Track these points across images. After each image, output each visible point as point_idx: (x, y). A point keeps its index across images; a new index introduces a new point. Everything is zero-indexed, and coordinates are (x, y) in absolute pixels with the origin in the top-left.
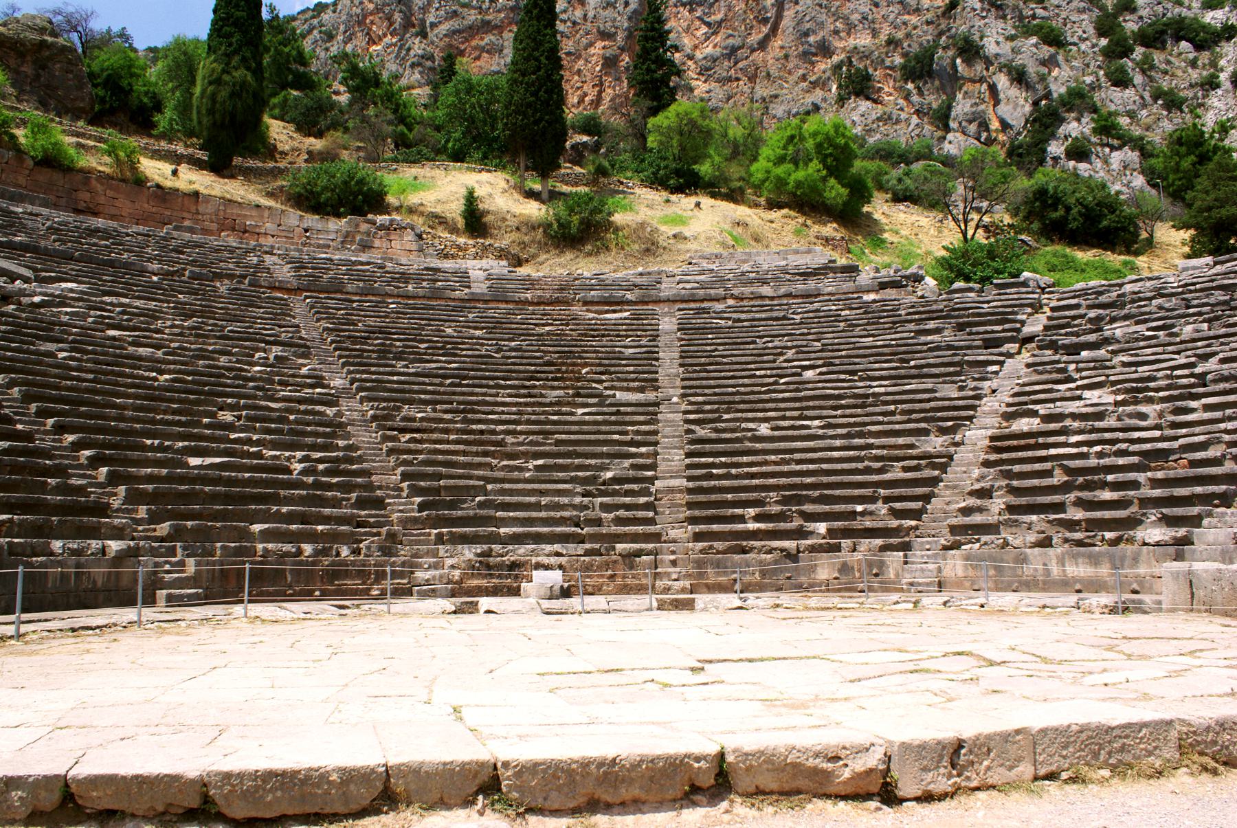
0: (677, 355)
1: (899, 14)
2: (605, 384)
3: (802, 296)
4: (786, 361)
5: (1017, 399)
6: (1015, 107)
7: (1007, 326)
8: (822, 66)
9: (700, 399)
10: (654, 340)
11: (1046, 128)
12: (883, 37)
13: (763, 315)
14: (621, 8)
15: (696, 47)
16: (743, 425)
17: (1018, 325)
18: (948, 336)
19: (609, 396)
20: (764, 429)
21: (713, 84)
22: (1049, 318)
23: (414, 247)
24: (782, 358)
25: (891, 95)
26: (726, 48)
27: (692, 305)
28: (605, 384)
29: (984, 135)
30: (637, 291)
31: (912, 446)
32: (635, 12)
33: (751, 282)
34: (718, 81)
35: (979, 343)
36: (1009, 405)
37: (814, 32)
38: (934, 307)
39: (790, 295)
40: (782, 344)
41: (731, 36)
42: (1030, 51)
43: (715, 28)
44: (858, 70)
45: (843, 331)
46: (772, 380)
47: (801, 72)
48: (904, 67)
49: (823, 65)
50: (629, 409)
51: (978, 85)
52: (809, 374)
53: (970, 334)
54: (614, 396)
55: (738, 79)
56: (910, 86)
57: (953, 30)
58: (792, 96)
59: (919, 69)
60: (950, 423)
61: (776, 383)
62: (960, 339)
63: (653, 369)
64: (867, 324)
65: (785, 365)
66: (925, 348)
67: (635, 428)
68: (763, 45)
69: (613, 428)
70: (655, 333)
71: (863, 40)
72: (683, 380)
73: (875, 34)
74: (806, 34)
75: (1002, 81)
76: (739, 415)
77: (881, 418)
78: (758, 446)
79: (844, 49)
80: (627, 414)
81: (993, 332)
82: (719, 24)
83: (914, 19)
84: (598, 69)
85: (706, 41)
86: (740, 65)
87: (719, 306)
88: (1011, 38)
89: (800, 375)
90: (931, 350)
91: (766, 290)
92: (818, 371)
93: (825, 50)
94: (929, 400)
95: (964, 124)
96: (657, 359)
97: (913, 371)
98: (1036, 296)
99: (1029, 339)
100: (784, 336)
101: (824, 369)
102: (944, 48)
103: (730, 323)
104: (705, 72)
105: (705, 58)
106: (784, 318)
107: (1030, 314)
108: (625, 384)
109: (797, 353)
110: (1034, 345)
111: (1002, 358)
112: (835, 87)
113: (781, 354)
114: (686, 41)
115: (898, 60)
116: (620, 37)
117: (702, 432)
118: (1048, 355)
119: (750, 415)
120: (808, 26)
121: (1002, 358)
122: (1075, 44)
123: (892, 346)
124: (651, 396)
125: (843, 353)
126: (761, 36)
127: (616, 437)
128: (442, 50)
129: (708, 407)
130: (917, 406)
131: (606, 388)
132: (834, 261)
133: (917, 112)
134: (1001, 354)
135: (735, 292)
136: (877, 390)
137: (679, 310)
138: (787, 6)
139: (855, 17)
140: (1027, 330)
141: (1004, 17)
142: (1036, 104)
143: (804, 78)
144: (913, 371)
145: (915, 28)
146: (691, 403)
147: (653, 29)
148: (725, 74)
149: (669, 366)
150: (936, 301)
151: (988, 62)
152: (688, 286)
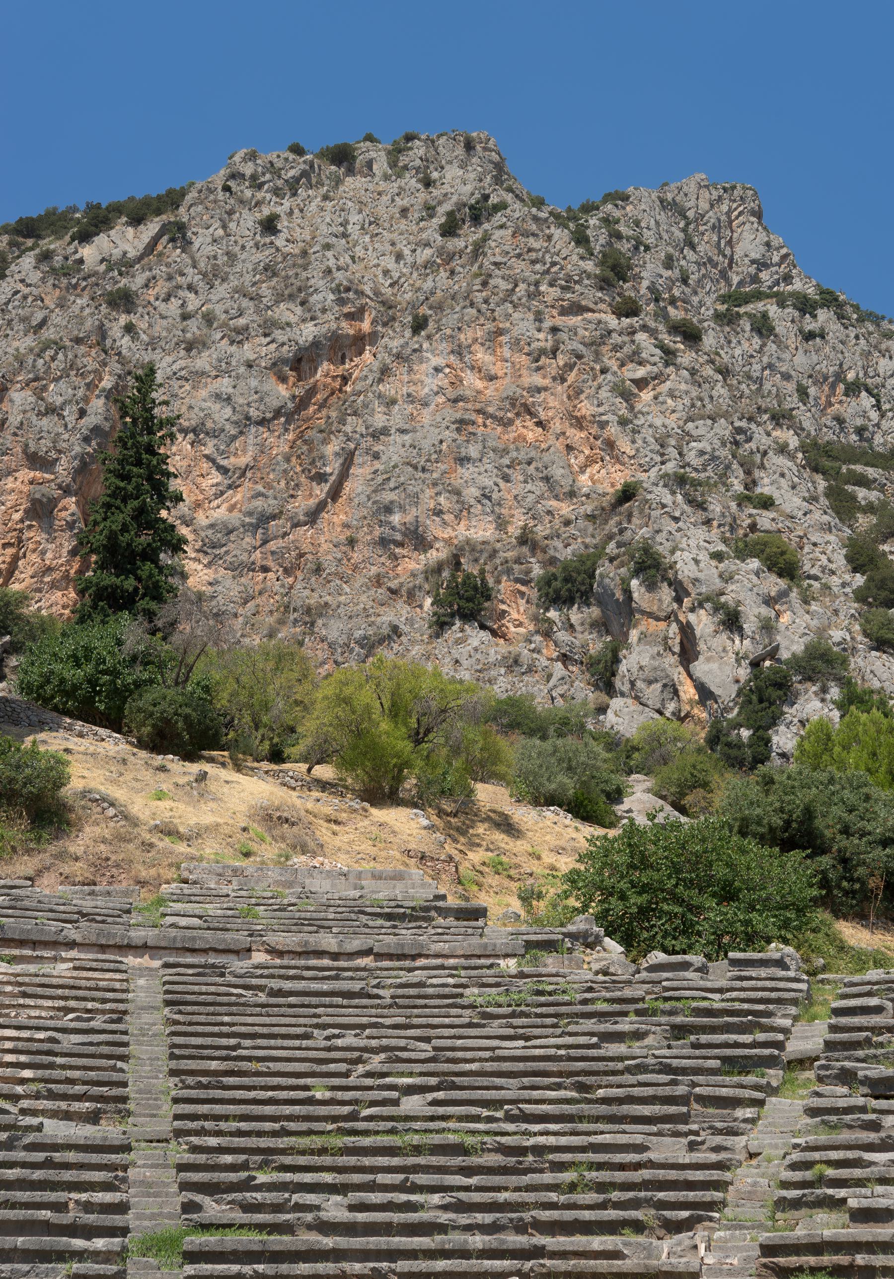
0: (162, 1051)
1: (541, 497)
2: (25, 1104)
3: (390, 956)
4: (369, 1075)
5: (798, 1176)
6: (723, 667)
7: (761, 1037)
8: (412, 565)
9: (213, 1141)
10: (119, 1021)
11: (771, 704)
12: (514, 530)
13: (325, 987)
14: (71, 419)
15: (198, 505)
16: (296, 1198)
17: (780, 1037)
18: (654, 1046)
19: (29, 1129)
20: (335, 1208)
21: (222, 571)
22: (833, 1029)
24: (361, 1069)
25: (520, 625)
26: (250, 514)
27: (190, 959)
28: (25, 1104)
29: (671, 707)
30: (83, 924)
31: (616, 1255)
32: (96, 430)
33: (300, 923)
35: (714, 1064)
36: (785, 1185)
37: (402, 509)
38: (628, 993)
39: (368, 952)
40: (362, 1043)
41: (260, 494)
42: (749, 584)
43: (233, 478)
44: (468, 576)
45: (470, 1025)
46: (346, 1110)
47: (374, 570)
48: (548, 581)
49: (413, 564)
50: (72, 1156)
51: (662, 625)
52: (412, 1104)
53: (696, 1046)
54: (39, 1128)
55: (265, 569)
56: (552, 614)
57: (629, 533)
58: (353, 608)
59: (568, 587)
60: (685, 1214)
61: (353, 1117)
62: (680, 1053)
63: (115, 1076)
64: (513, 1015)
65: (369, 1082)
66: (620, 1066)
67: (84, 1196)
68: (313, 516)
69: (38, 1196)
70: (121, 1007)
71: (481, 530)
72: (176, 1101)
73: (502, 524)
74: (388, 509)
75: (703, 622)
76: (288, 1177)
77: (553, 1196)
78: (329, 1242)
79: (448, 542)
80: (67, 1166)
81: (737, 1045)
83: (565, 509)
84: (17, 516)
85: (217, 496)
86: (272, 545)
87: (238, 965)
88: (718, 556)
89: (396, 1103)
90: (628, 1070)
91: (328, 941)
92: (430, 1097)
93: (419, 540)
94: (637, 1166)
95: (640, 684)
96: (123, 1058)
97: (603, 1109)
98: (803, 986)
99: (803, 1062)
101: (440, 1095)
102: (611, 560)
103: (262, 998)
104: (210, 549)
105: (212, 526)
106: (362, 994)
107: (796, 1018)
108: (63, 1105)
109: (390, 1060)
110: (810, 1074)
111: (759, 1095)
112: (428, 601)
113: (358, 1061)
115: (537, 571)
116: (64, 469)
117: (213, 1208)
118: (839, 1095)
119: (308, 1178)
121: (759, 1095)
122: (816, 578)
123: (559, 1059)
124: (108, 1130)
125: (474, 1067)
126: (312, 502)
127: (45, 1214)
129: (228, 1159)
130: (620, 1176)
131: (23, 1112)
132: (443, 897)
133: (565, 658)
134: (757, 1087)
135: (274, 939)
136: (541, 1140)
137: (166, 965)
138: (358, 459)
139: (471, 493)
140: (795, 1047)
141: (708, 522)
142: (755, 664)
143: (378, 581)
144: (603, 1109)
145: (567, 523)
146: (195, 1149)
147: (139, 463)
148: (244, 557)
149: (148, 1070)
150: (629, 982)
151: (680, 592)
152: (183, 922)
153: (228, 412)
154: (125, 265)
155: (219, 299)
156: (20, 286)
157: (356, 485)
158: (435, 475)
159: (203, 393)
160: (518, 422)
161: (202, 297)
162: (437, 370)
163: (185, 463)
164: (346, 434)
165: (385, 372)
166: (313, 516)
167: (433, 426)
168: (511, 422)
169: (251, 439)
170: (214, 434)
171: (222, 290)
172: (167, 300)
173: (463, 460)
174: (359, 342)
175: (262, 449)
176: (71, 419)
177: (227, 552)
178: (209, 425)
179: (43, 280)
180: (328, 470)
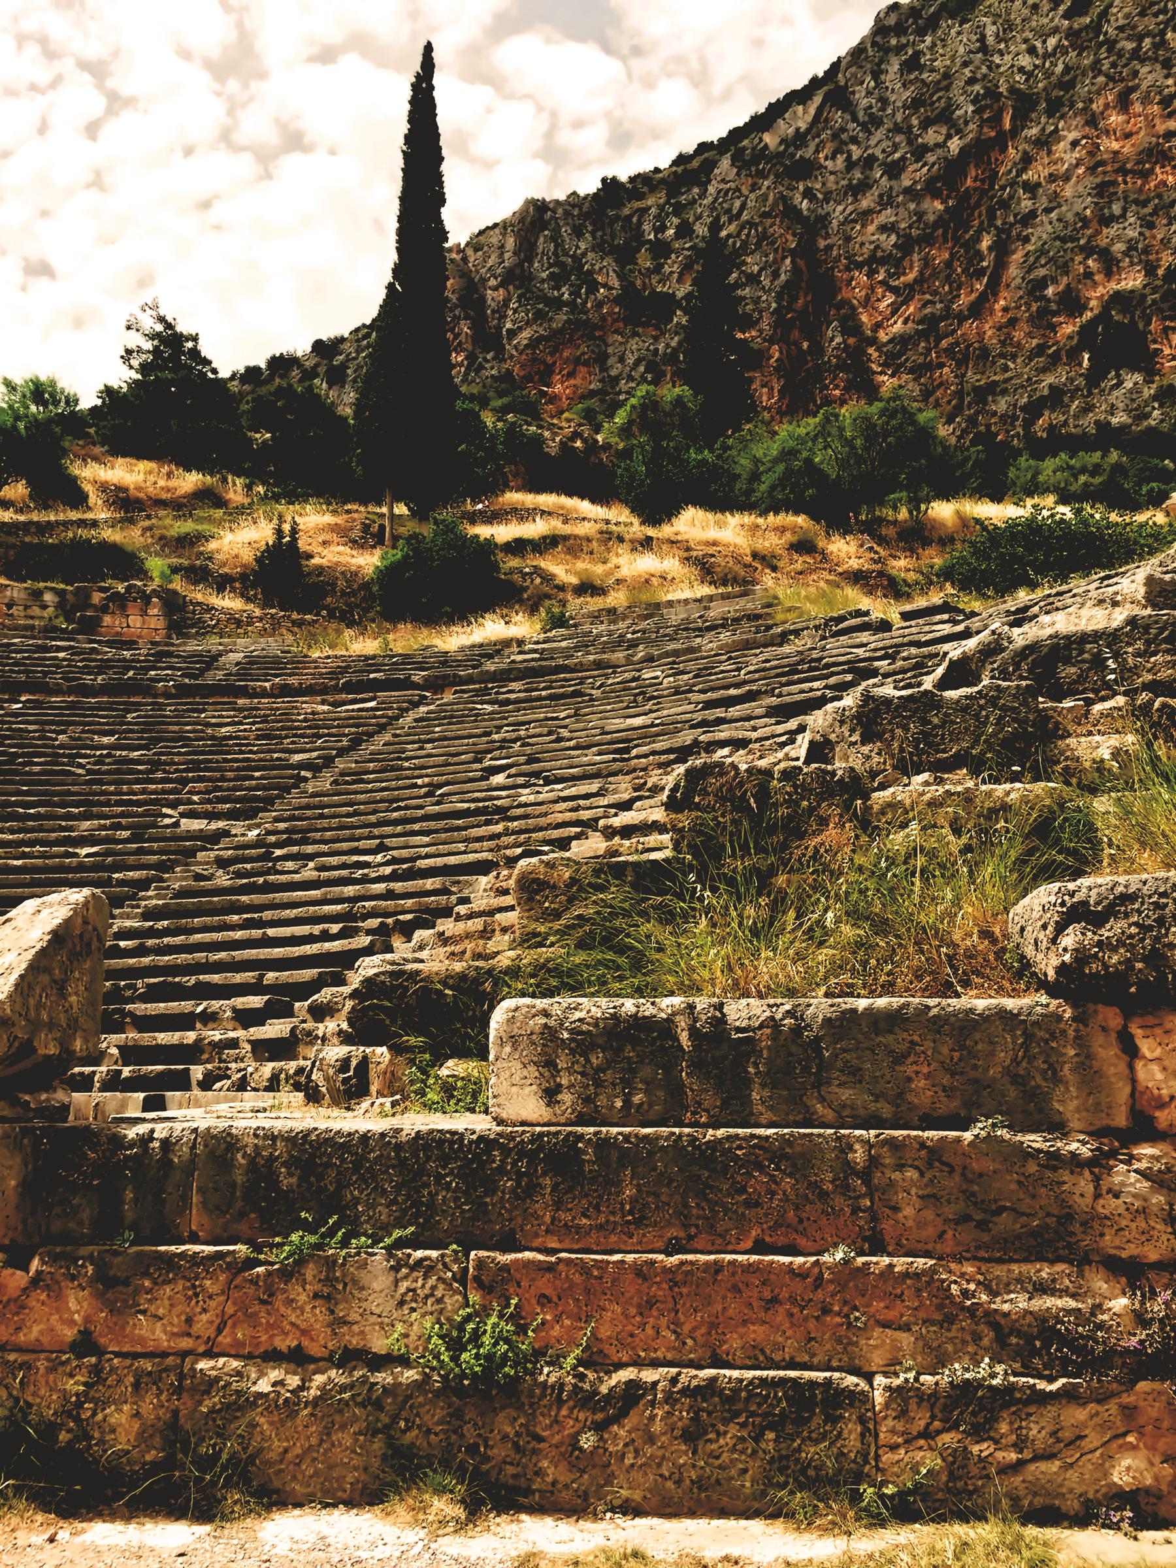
8: (1069, 329)
21: (905, 377)
23: (161, 623)
34: (911, 371)
37: (1055, 281)
43: (905, 295)
68: (978, 309)
71: (1132, 280)
81: (812, 690)
82: (910, 286)
85: (893, 314)
86: (944, 343)
100: (529, 723)
105: (890, 341)
114: (864, 318)
120: (1042, 272)
126: (974, 296)
128: (523, 366)
153: (893, 238)
154: (800, 139)
155: (878, 143)
156: (722, 186)
157: (1013, 271)
158: (1082, 242)
159: (871, 228)
160: (1158, 170)
161: (863, 145)
162: (1075, 144)
163: (863, 293)
164: (997, 228)
165: (1027, 161)
166: (978, 309)
167: (1077, 196)
168: (1151, 171)
169: (916, 257)
170: (882, 261)
171: (879, 134)
172: (834, 158)
173: (1107, 221)
174: (1001, 142)
175: (926, 262)
176: (766, 283)
177: (907, 360)
178: (879, 254)
179: (738, 174)
180: (985, 264)
